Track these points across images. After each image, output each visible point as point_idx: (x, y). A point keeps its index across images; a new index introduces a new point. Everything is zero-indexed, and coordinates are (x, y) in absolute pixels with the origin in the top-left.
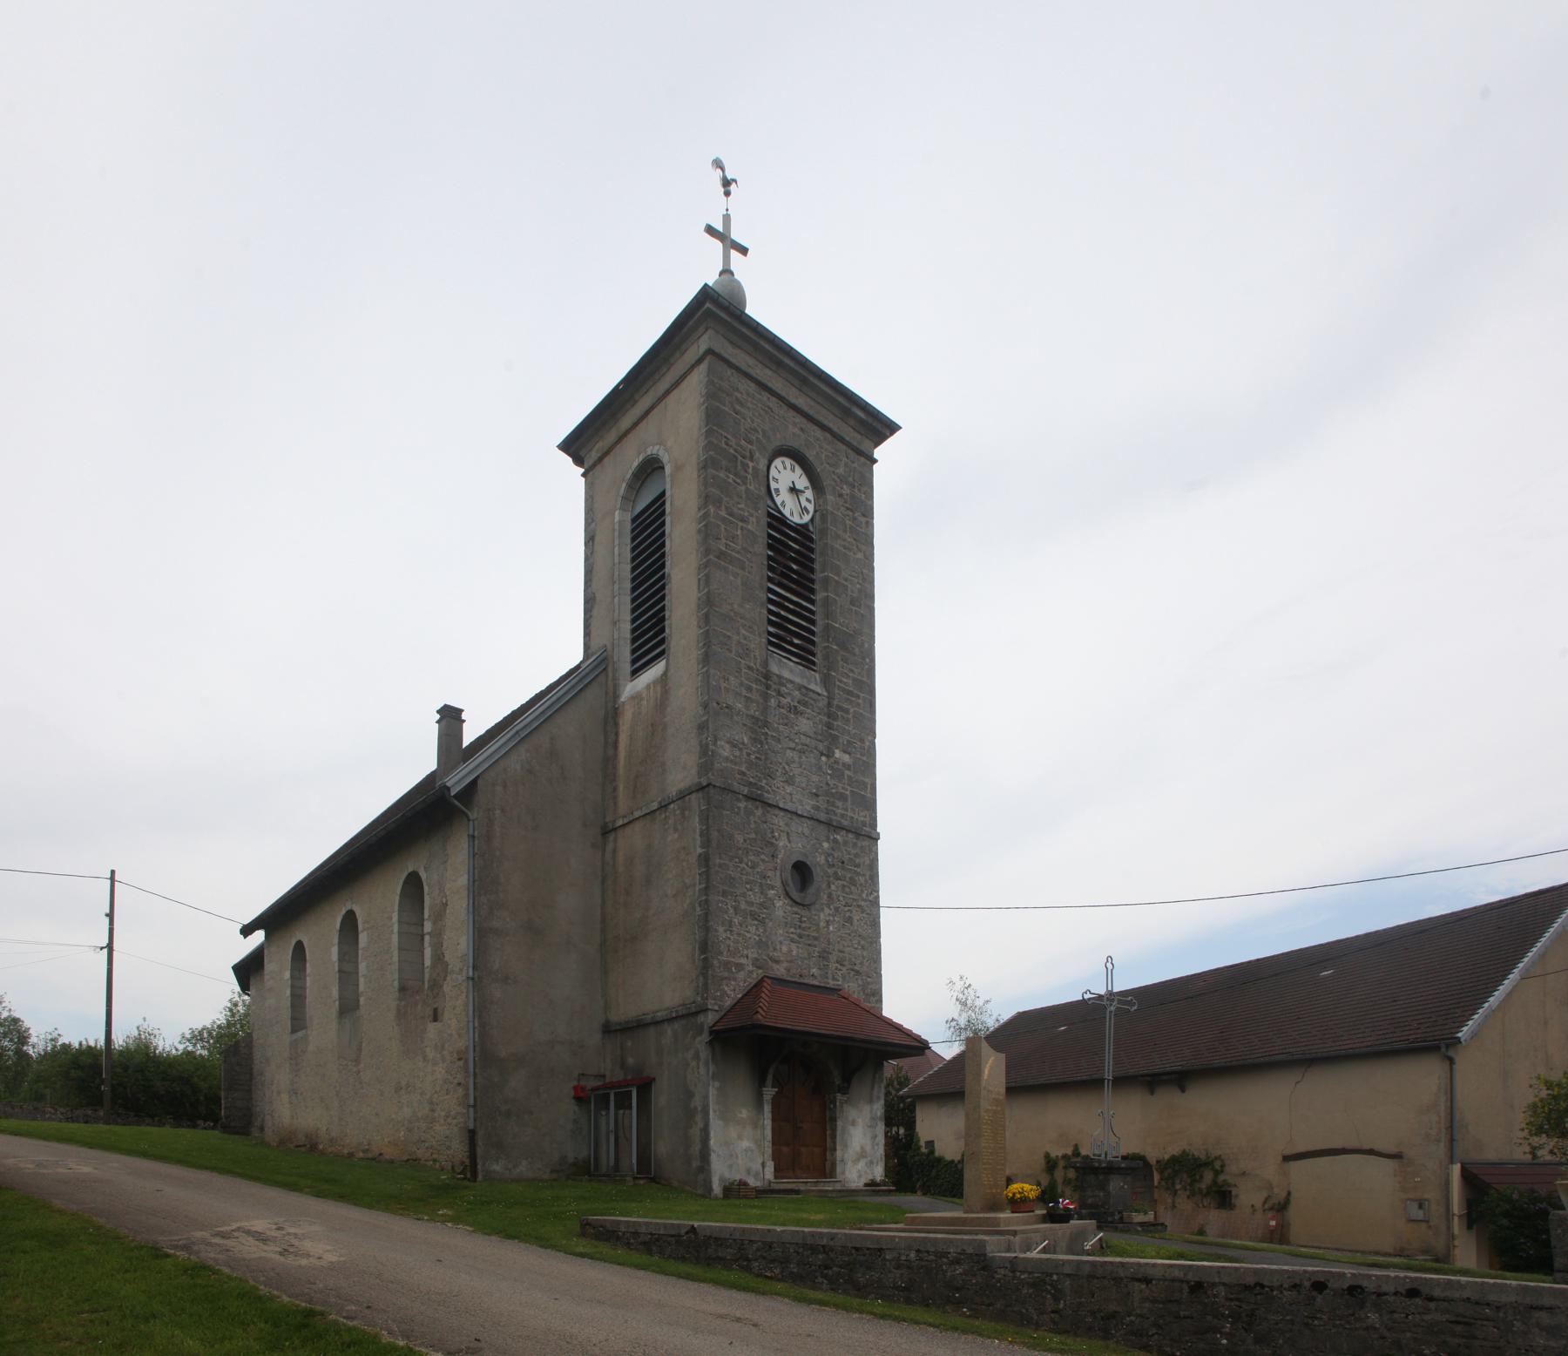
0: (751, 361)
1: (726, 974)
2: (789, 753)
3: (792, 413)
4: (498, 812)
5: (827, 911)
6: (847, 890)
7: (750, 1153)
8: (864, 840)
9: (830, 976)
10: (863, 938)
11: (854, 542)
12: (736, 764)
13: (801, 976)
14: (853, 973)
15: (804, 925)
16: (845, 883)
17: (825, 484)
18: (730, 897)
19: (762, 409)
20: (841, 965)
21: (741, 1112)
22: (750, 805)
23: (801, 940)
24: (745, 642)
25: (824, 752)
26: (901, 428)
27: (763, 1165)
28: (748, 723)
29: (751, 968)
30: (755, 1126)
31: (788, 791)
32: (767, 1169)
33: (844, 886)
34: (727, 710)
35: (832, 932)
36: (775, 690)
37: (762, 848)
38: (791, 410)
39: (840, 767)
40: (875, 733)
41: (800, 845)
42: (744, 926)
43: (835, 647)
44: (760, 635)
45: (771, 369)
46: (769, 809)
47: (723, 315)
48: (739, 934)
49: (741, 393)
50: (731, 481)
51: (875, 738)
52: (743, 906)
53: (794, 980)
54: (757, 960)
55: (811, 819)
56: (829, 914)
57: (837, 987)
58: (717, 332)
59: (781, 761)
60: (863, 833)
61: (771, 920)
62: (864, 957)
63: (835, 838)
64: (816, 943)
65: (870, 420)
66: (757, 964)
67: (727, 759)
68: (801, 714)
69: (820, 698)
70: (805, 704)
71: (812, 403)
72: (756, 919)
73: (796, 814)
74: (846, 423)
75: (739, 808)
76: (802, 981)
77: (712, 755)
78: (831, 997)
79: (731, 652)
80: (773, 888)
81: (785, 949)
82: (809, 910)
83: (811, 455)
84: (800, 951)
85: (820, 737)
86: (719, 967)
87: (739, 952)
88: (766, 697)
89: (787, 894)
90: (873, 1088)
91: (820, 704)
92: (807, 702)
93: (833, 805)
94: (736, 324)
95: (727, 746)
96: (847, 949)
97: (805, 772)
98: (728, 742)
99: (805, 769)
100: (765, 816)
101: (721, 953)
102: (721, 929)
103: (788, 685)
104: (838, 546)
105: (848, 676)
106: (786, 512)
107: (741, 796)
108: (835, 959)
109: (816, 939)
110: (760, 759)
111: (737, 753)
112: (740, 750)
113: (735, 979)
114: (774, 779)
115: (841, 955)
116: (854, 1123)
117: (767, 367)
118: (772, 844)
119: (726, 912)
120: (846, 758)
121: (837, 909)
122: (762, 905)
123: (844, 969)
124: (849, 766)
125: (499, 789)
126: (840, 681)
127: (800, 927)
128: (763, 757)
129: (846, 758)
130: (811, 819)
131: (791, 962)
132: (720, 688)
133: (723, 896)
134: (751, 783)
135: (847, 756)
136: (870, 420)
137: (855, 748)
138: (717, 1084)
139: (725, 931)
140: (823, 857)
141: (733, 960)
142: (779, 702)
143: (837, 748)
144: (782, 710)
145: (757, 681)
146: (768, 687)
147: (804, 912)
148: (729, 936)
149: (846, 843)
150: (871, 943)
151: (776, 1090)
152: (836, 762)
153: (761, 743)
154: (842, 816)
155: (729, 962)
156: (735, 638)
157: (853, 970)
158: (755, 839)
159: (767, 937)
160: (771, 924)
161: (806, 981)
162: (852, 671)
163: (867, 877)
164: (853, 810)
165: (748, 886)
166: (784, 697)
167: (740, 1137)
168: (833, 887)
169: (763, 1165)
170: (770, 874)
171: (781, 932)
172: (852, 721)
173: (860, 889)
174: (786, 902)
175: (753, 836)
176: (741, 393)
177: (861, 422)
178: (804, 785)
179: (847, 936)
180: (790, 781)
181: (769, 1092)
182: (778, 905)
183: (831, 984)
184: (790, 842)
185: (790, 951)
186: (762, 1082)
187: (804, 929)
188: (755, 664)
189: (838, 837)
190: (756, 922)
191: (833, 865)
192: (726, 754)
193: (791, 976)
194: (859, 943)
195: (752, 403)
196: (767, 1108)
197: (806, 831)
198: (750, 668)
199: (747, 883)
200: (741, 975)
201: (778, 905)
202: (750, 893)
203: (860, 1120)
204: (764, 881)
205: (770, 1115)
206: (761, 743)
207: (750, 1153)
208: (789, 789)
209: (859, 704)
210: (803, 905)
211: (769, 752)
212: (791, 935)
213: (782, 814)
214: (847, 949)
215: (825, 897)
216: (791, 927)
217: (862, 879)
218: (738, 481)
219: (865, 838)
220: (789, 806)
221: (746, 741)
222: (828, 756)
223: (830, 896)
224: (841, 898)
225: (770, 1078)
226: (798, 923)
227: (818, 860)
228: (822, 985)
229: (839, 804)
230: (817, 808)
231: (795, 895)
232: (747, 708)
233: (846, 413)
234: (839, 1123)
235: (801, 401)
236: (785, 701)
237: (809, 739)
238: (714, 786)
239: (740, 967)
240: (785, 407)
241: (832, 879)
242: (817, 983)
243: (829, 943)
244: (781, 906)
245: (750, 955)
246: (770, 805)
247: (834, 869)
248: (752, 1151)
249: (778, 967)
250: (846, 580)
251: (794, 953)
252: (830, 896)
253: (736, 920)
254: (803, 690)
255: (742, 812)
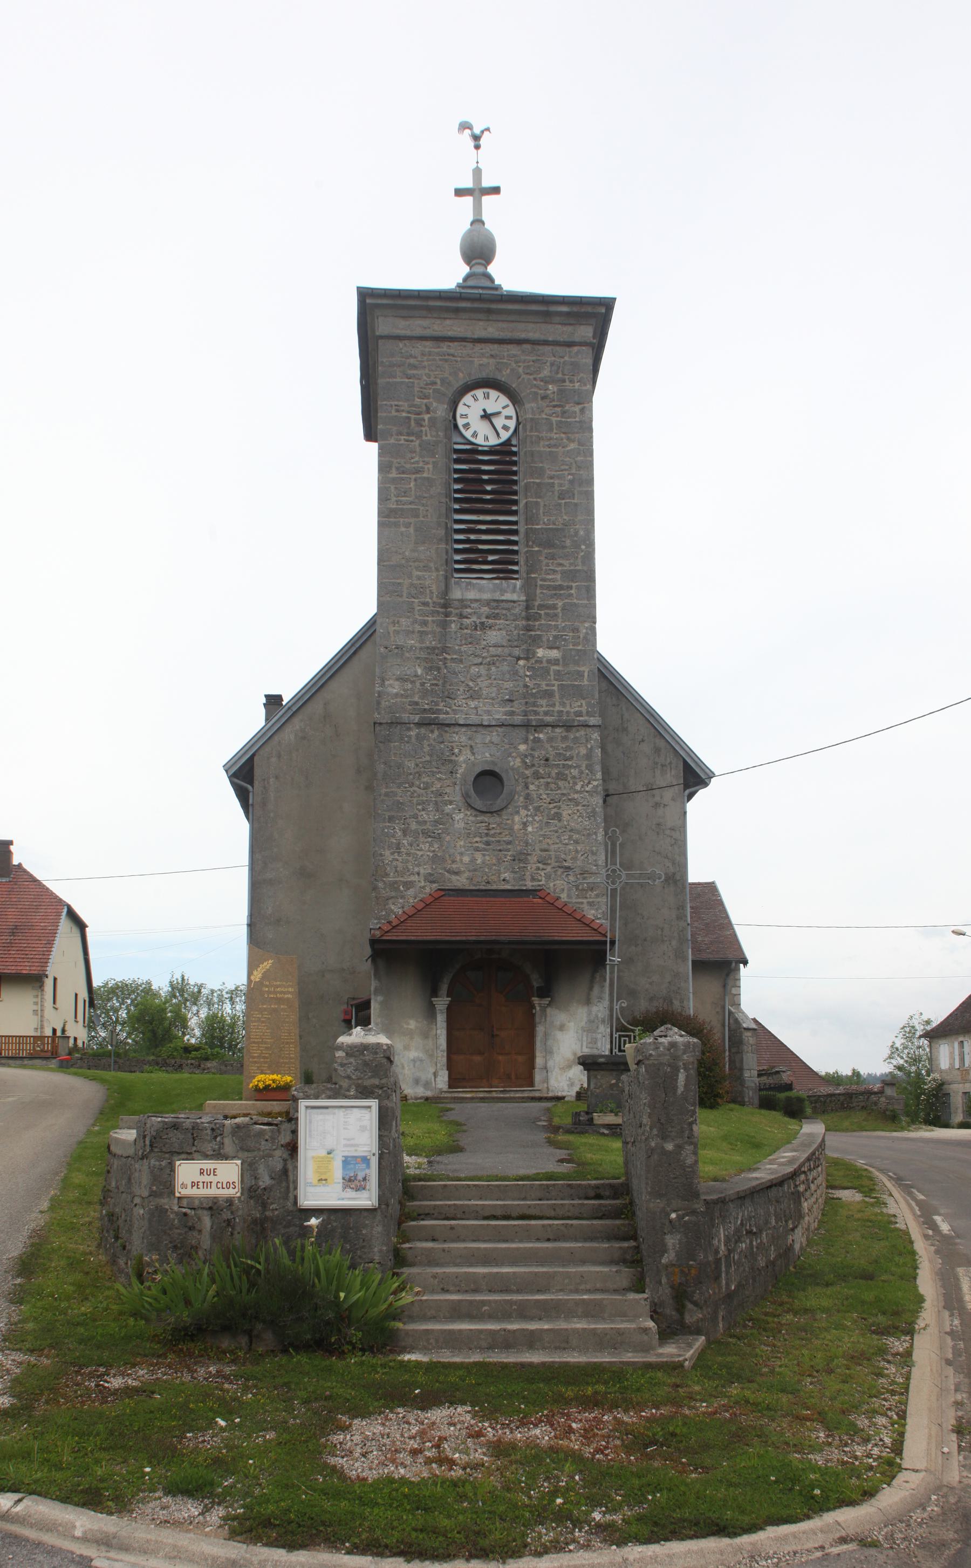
0: (425, 323)
1: (393, 894)
2: (474, 670)
3: (478, 347)
4: (272, 780)
5: (523, 812)
6: (553, 786)
7: (418, 1063)
8: (578, 731)
9: (528, 877)
10: (578, 832)
11: (563, 436)
12: (407, 697)
13: (488, 883)
14: (561, 870)
15: (492, 832)
16: (549, 780)
17: (522, 395)
18: (397, 821)
19: (441, 360)
20: (544, 864)
21: (408, 1024)
22: (423, 730)
23: (489, 847)
24: (419, 582)
25: (522, 656)
26: (615, 299)
27: (435, 1075)
28: (423, 655)
29: (423, 884)
30: (426, 1036)
31: (473, 706)
32: (439, 1079)
33: (548, 783)
34: (396, 651)
35: (530, 833)
36: (457, 614)
37: (438, 768)
38: (476, 344)
39: (545, 665)
40: (595, 617)
41: (487, 755)
42: (415, 845)
43: (536, 549)
44: (437, 570)
45: (450, 319)
46: (447, 729)
47: (385, 301)
48: (408, 854)
49: (415, 357)
50: (402, 442)
51: (595, 623)
52: (414, 826)
53: (477, 888)
54: (431, 875)
55: (502, 725)
56: (527, 815)
57: (539, 888)
58: (385, 316)
59: (463, 679)
60: (576, 724)
61: (448, 834)
62: (577, 851)
63: (535, 738)
64: (509, 847)
65: (575, 309)
66: (430, 879)
67: (397, 695)
68: (490, 628)
69: (515, 605)
70: (496, 617)
71: (505, 325)
72: (430, 836)
73: (482, 725)
74: (551, 323)
75: (410, 737)
76: (489, 887)
77: (379, 696)
78: (525, 899)
79: (401, 596)
80: (451, 803)
81: (466, 859)
82: (500, 816)
83: (503, 376)
84: (487, 858)
85: (515, 643)
86: (384, 889)
87: (408, 871)
88: (444, 625)
89: (470, 806)
90: (591, 988)
91: (517, 611)
92: (498, 614)
93: (534, 705)
94: (400, 302)
95: (397, 683)
96: (552, 847)
97: (495, 682)
98: (397, 680)
99: (495, 679)
100: (442, 736)
101: (387, 875)
102: (387, 853)
103: (472, 605)
104: (542, 449)
105: (554, 571)
106: (480, 440)
107: (412, 725)
108: (535, 859)
109: (509, 843)
110: (437, 685)
111: (410, 686)
112: (413, 682)
113: (402, 897)
114: (455, 699)
115: (544, 854)
116: (562, 1028)
117: (445, 319)
118: (451, 761)
119: (393, 836)
120: (554, 654)
121: (537, 809)
122: (437, 822)
123: (549, 869)
124: (558, 660)
125: (274, 760)
126: (544, 580)
127: (487, 835)
128: (440, 683)
129: (554, 654)
130: (502, 725)
131: (475, 870)
132: (389, 633)
133: (389, 822)
134: (425, 709)
135: (555, 651)
136: (575, 309)
137: (565, 640)
138: (380, 998)
139: (392, 854)
140: (518, 760)
141: (402, 879)
142: (462, 624)
143: (539, 647)
144: (466, 631)
145: (433, 613)
146: (447, 615)
147: (493, 820)
148: (397, 857)
149: (550, 740)
150: (589, 835)
151: (450, 999)
152: (539, 661)
153: (439, 669)
154: (546, 713)
155: (396, 882)
156: (407, 582)
157: (559, 867)
158: (430, 762)
159: (444, 851)
160: (448, 838)
161: (494, 887)
162: (561, 565)
163: (583, 768)
164: (564, 705)
165: (420, 807)
166: (467, 618)
167: (407, 1048)
168: (532, 787)
169: (435, 1075)
170: (448, 790)
171: (462, 843)
172: (561, 615)
173: (571, 782)
174: (469, 813)
175: (428, 758)
176: (415, 357)
177: (568, 314)
178: (493, 695)
179: (553, 833)
180: (474, 695)
181: (442, 1003)
182: (457, 818)
183: (530, 885)
184: (473, 754)
185: (473, 860)
186: (435, 992)
187: (493, 836)
188: (431, 598)
189: (541, 736)
190: (430, 839)
191: (533, 765)
192: (395, 691)
193: (475, 885)
194: (570, 838)
195: (428, 360)
196: (441, 1019)
197: (496, 739)
198: (425, 604)
199: (419, 804)
200: (411, 892)
201: (457, 818)
202: (423, 813)
203: (572, 1024)
204: (439, 799)
205: (445, 1025)
206: (439, 669)
207: (418, 1063)
208: (472, 704)
209: (571, 595)
210: (491, 813)
211: (448, 675)
212: (477, 845)
213: (464, 729)
214: (552, 847)
215: (521, 799)
216: (475, 837)
217: (575, 772)
218: (411, 438)
219: (579, 728)
220: (474, 719)
221: (419, 671)
222: (527, 659)
223: (527, 797)
224: (545, 796)
225: (444, 988)
226: (486, 831)
227: (512, 764)
228: (516, 888)
229: (543, 702)
230: (512, 713)
231: (478, 804)
232: (422, 641)
233: (547, 316)
234: (540, 1030)
235: (492, 330)
236: (467, 621)
237: (500, 649)
238: (380, 724)
239: (409, 885)
240: (470, 345)
241: (529, 780)
242: (509, 887)
243: (527, 843)
244: (461, 819)
245: (422, 871)
246: (449, 725)
247: (534, 768)
248: (421, 1061)
249: (458, 878)
250: (551, 478)
251: (479, 861)
252: (527, 797)
253: (405, 842)
254: (494, 604)
255: (413, 740)
